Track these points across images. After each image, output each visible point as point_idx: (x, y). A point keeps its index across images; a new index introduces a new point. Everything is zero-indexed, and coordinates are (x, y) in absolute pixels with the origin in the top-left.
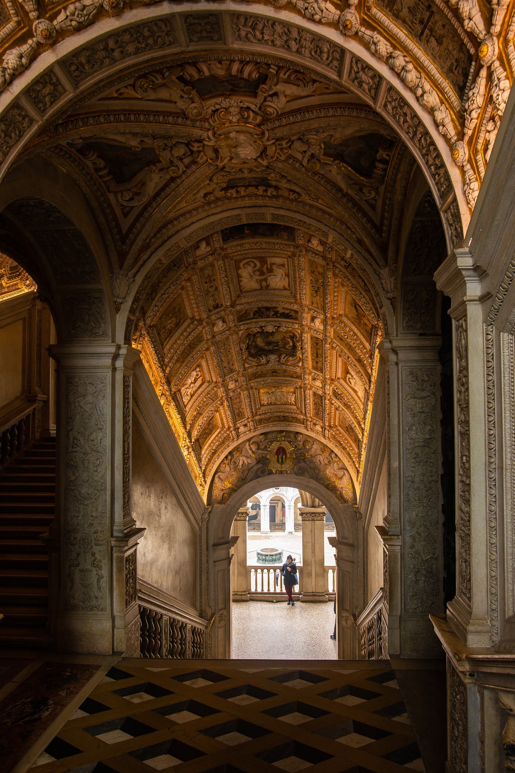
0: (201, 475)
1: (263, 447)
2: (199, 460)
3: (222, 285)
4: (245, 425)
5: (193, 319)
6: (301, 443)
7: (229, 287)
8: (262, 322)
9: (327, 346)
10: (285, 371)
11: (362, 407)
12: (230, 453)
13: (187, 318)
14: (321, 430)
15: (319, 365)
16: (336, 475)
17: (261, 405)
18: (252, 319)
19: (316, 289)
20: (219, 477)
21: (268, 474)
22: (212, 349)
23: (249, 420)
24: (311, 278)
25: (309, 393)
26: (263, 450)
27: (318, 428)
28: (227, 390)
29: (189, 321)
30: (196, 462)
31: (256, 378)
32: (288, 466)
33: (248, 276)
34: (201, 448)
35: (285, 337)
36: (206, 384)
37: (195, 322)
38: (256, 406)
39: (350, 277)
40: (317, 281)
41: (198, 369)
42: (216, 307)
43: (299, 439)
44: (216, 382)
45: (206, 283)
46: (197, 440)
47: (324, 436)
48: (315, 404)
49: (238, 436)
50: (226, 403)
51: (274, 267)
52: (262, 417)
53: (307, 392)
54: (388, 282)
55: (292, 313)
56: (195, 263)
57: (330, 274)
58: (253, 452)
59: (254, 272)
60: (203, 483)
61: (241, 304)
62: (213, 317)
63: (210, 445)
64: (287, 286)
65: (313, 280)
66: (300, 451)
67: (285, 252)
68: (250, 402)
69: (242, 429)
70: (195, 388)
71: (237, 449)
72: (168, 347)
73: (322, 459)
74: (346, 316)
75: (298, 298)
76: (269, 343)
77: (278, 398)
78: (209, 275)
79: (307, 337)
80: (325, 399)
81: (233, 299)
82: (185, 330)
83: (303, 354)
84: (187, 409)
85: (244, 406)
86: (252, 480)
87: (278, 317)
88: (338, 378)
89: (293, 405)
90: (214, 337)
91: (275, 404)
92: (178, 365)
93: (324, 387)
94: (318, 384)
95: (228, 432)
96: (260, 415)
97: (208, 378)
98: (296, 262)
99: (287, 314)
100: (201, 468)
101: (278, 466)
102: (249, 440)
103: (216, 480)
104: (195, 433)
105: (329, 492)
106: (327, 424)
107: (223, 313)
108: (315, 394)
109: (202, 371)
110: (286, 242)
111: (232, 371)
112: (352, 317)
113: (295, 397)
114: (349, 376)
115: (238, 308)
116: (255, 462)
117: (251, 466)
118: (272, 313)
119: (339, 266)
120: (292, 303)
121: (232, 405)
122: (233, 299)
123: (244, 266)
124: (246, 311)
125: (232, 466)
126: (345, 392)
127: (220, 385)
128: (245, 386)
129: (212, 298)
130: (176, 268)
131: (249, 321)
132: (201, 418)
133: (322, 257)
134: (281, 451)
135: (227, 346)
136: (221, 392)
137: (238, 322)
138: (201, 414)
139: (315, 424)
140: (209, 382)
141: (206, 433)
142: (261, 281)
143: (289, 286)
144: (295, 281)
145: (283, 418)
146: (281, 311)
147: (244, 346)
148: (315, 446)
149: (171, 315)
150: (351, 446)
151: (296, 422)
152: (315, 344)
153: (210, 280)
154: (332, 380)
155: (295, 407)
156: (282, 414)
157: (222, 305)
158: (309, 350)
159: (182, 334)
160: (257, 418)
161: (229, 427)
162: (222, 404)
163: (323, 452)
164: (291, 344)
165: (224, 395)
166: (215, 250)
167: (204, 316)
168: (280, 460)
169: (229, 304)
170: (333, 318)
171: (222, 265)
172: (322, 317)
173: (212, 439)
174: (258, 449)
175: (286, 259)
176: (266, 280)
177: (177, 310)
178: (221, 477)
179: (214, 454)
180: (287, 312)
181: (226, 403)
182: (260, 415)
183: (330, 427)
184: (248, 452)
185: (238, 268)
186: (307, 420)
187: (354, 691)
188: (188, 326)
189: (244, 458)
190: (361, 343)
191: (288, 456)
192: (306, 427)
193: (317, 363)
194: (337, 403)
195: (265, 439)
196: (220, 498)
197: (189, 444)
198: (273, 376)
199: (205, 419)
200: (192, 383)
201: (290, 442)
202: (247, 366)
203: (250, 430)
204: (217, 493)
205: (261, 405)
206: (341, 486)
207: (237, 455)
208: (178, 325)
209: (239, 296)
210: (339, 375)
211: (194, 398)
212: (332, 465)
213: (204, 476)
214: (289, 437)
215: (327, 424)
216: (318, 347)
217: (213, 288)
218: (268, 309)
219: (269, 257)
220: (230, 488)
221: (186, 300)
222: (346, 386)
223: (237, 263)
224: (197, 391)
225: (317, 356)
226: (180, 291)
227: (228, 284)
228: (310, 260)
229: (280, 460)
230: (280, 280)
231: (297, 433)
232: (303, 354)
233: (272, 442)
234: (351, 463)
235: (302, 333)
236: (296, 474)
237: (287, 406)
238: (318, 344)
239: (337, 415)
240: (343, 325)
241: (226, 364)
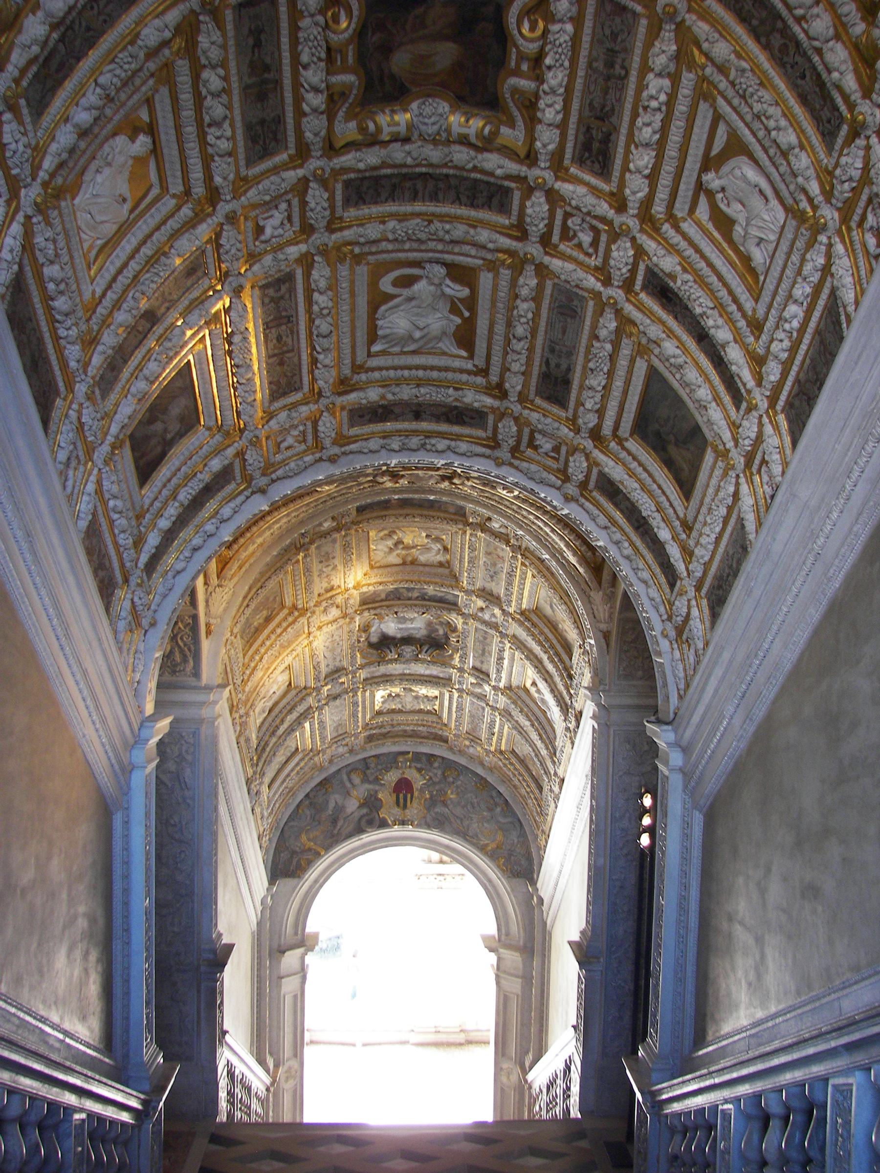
1: (371, 778)
5: (295, 607)
6: (439, 772)
26: (370, 782)
29: (286, 611)
32: (414, 809)
33: (386, 550)
37: (296, 614)
40: (494, 565)
54: (601, 610)
66: (437, 787)
82: (279, 625)
101: (396, 811)
168: (401, 801)
180: (440, 594)
187: (535, 1152)
188: (285, 619)
191: (416, 794)
201: (419, 770)
211: (273, 714)
229: (401, 801)
231: (432, 755)
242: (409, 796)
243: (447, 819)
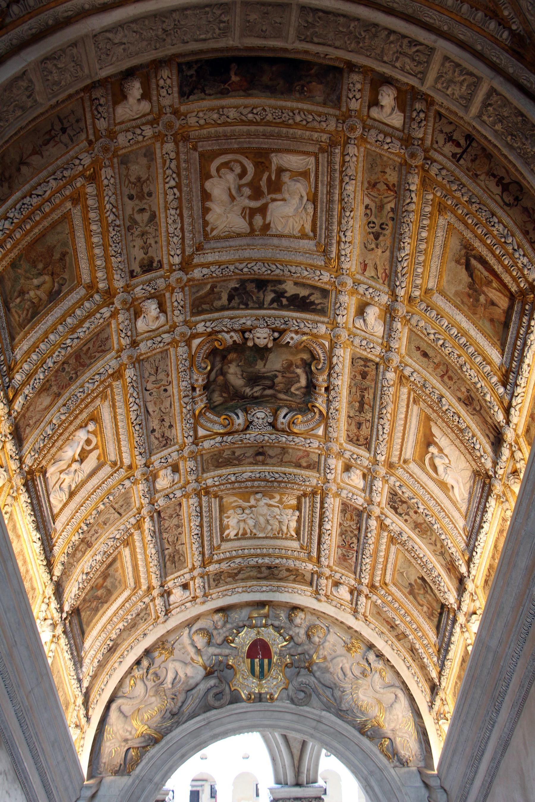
0: (80, 700)
1: (219, 640)
2: (78, 661)
3: (166, 209)
4: (185, 586)
5: (91, 287)
6: (302, 632)
7: (181, 215)
8: (245, 317)
9: (391, 376)
10: (284, 450)
11: (461, 523)
12: (147, 652)
13: (79, 284)
14: (348, 597)
15: (365, 431)
16: (379, 702)
17: (223, 540)
18: (223, 308)
19: (377, 228)
20: (120, 710)
21: (231, 703)
22: (129, 373)
23: (196, 573)
24: (367, 201)
25: (333, 505)
26: (219, 645)
27: (344, 593)
28: (152, 491)
29: (82, 292)
30: (70, 664)
31: (218, 466)
34: (83, 633)
35: (290, 364)
36: (107, 470)
37: (97, 297)
38: (211, 540)
39: (465, 179)
40: (381, 207)
41: (91, 427)
42: (148, 266)
43: (298, 621)
44: (130, 467)
45: (131, 197)
46: (76, 612)
47: (355, 612)
48: (341, 534)
49: (167, 612)
50: (147, 525)
51: (286, 177)
52: (224, 566)
53: (330, 500)
55: (316, 298)
56: (112, 135)
57: (414, 183)
58: (198, 651)
59: (239, 188)
60: (83, 720)
61: (202, 265)
62: (138, 291)
63: (104, 627)
64: (308, 228)
65: (372, 206)
66: (300, 650)
67: (316, 135)
68: (201, 526)
69: (177, 595)
70: (81, 476)
71: (161, 643)
72: (25, 346)
73: (347, 666)
74: (442, 293)
75: (333, 255)
76: (253, 380)
77: (262, 520)
78: (139, 179)
79: (343, 357)
80: (369, 516)
81: (188, 251)
82: (70, 312)
83: (329, 402)
84: (59, 525)
85: (186, 538)
86: (192, 716)
87: (282, 307)
88: (405, 462)
89: (291, 538)
90: (134, 344)
91: (254, 537)
92: (46, 400)
93: (369, 488)
94: (356, 479)
95: (147, 600)
96: (219, 562)
97: (113, 456)
98: (338, 159)
99: (304, 298)
100: (80, 681)
102: (189, 624)
103: (113, 714)
104: (72, 591)
105: (366, 741)
106: (365, 581)
107: (161, 283)
108: (345, 508)
109: (100, 432)
110: (321, 109)
111: (166, 442)
112: (457, 294)
113: (299, 517)
114: (433, 449)
115: (197, 274)
116: (202, 672)
117: (192, 682)
118: (270, 296)
119: (440, 158)
120: (319, 268)
121: (161, 533)
122: (188, 251)
123: (218, 170)
124: (213, 287)
125: (150, 684)
126: (421, 492)
127: (138, 474)
128: (194, 485)
129: (139, 242)
130: (65, 138)
131: (216, 315)
132: (89, 553)
133: (400, 140)
134: (259, 649)
135: (161, 376)
136: (138, 492)
137: (193, 314)
138: (89, 545)
139: (337, 584)
140: (115, 464)
141: (97, 598)
142: (253, 212)
143: (314, 230)
144: (329, 211)
145: (266, 572)
146: (290, 289)
147: (200, 380)
148: (332, 638)
149: (40, 266)
150: (420, 628)
151: (294, 581)
152: (359, 377)
153: (140, 191)
154: (391, 466)
155: (295, 545)
156: (267, 560)
157: (161, 265)
158: (345, 392)
159: (62, 320)
160: (212, 568)
161: (150, 588)
162: (138, 526)
163: (349, 650)
164: (303, 382)
165: (145, 501)
166: (161, 113)
167: (119, 284)
168: (257, 669)
169: (177, 260)
170: (411, 299)
171: (173, 155)
172: (385, 299)
173: (110, 613)
174: (209, 643)
175: (312, 159)
176: (263, 210)
177: (57, 256)
178: (124, 708)
179: (112, 650)
180: (303, 292)
181: (147, 525)
182: (219, 562)
183: (372, 587)
184: (186, 652)
185: (205, 176)
186: (320, 575)
188: (79, 304)
189: (178, 666)
190: (480, 352)
191: (275, 659)
192: (317, 592)
193: (359, 425)
194: (395, 522)
195: (226, 622)
196: (119, 760)
197: (57, 615)
198: (256, 464)
199: (99, 558)
200: (74, 460)
201: (277, 629)
202: (201, 432)
203: (195, 598)
204: (113, 750)
205: (223, 540)
206: (393, 725)
207: (163, 658)
208: (54, 296)
209: (199, 248)
210: (408, 453)
211: (78, 499)
212: (369, 679)
213: (86, 703)
214: (277, 617)
215: (365, 581)
216: (367, 383)
217: (146, 216)
218: (262, 284)
219: (278, 151)
220: (142, 735)
221: (80, 234)
222: (424, 478)
223: (206, 158)
224: (83, 483)
225: (361, 410)
226: (69, 205)
227: (179, 208)
228: (368, 153)
229: (257, 669)
230: (296, 210)
231: (295, 608)
232: (329, 402)
233: (239, 629)
234: (415, 668)
235: (333, 346)
236: (292, 701)
237: (278, 542)
238: (366, 372)
239: (392, 556)
240: (434, 313)
241: (155, 424)
242: (266, 661)
243: (315, 691)
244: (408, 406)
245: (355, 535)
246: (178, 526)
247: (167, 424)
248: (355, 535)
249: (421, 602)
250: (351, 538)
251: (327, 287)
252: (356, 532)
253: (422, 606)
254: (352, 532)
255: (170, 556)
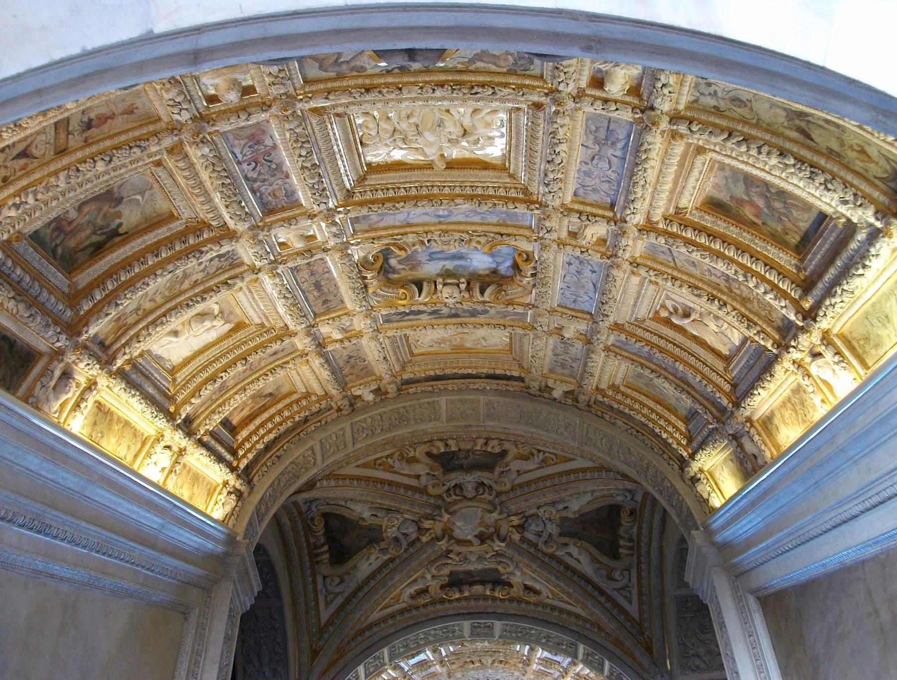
40: (352, 367)
152: (331, 297)
193: (312, 274)
244: (267, 317)
245: (255, 180)
246: (587, 174)
247: (573, 268)
248: (255, 180)
249: (86, 209)
250: (260, 174)
251: (387, 325)
252: (256, 185)
253: (79, 209)
254: (265, 180)
255: (613, 144)
